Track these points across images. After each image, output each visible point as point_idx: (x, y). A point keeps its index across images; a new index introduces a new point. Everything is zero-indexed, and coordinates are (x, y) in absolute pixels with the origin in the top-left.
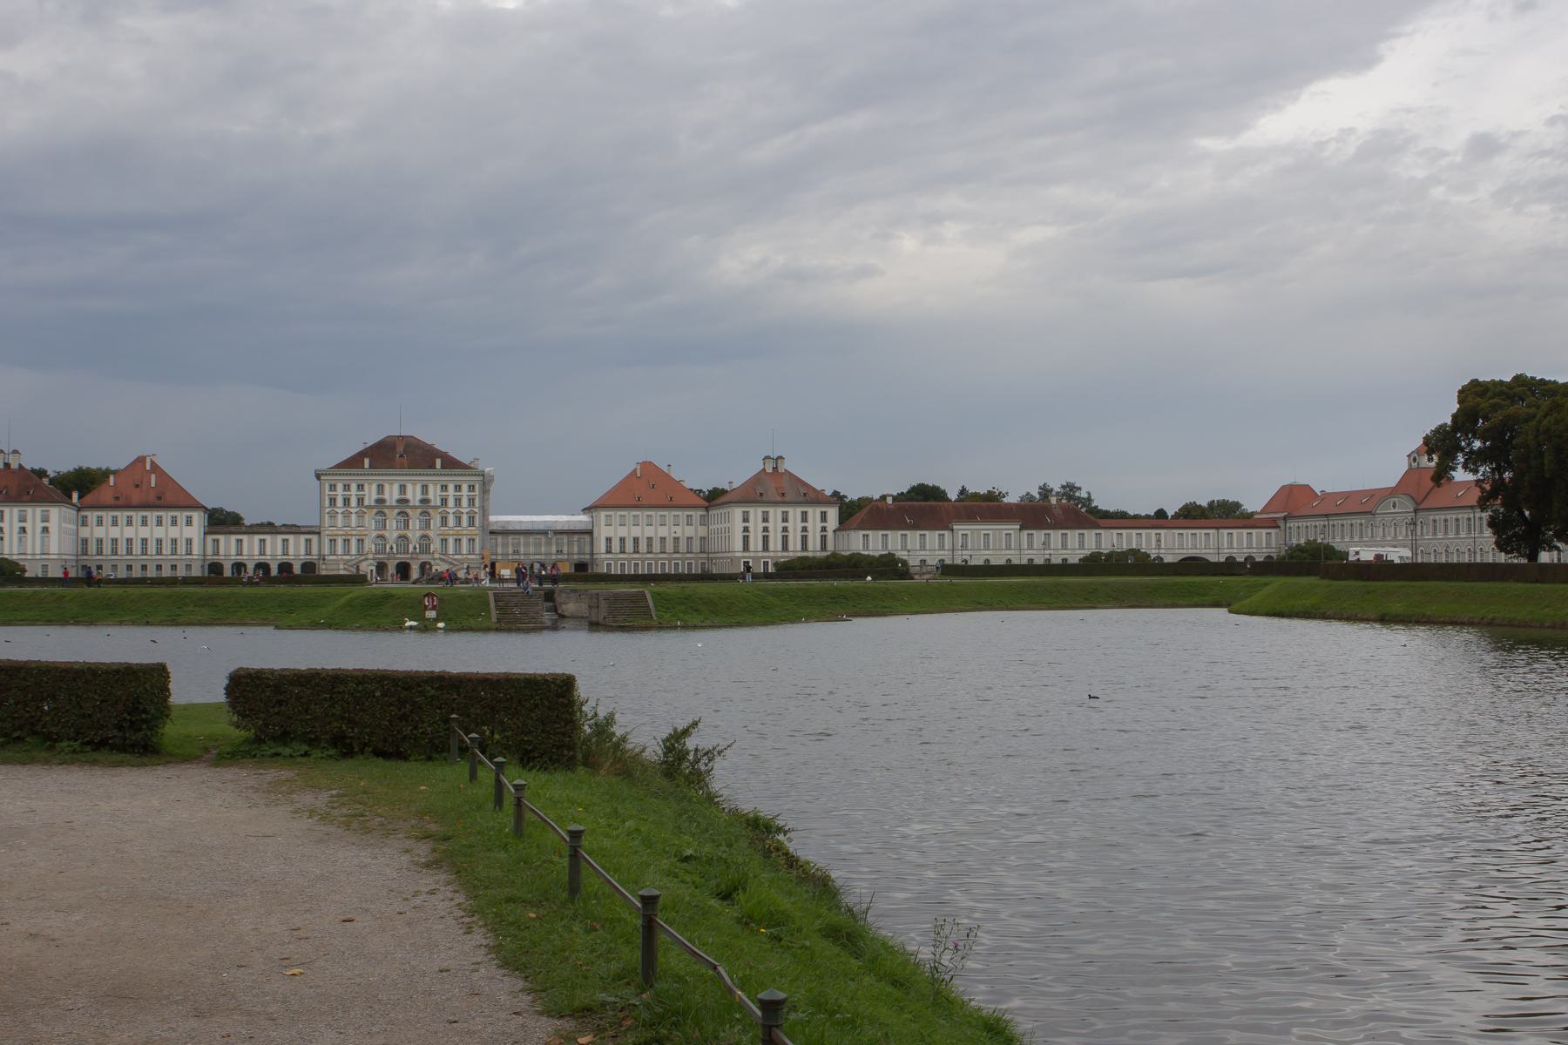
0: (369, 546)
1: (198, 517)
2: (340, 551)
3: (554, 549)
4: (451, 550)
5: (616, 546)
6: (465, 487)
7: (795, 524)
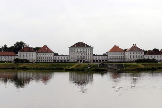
1: (53, 54)
2: (72, 58)
4: (88, 58)
5: (111, 58)
6: (89, 49)
7: (138, 54)
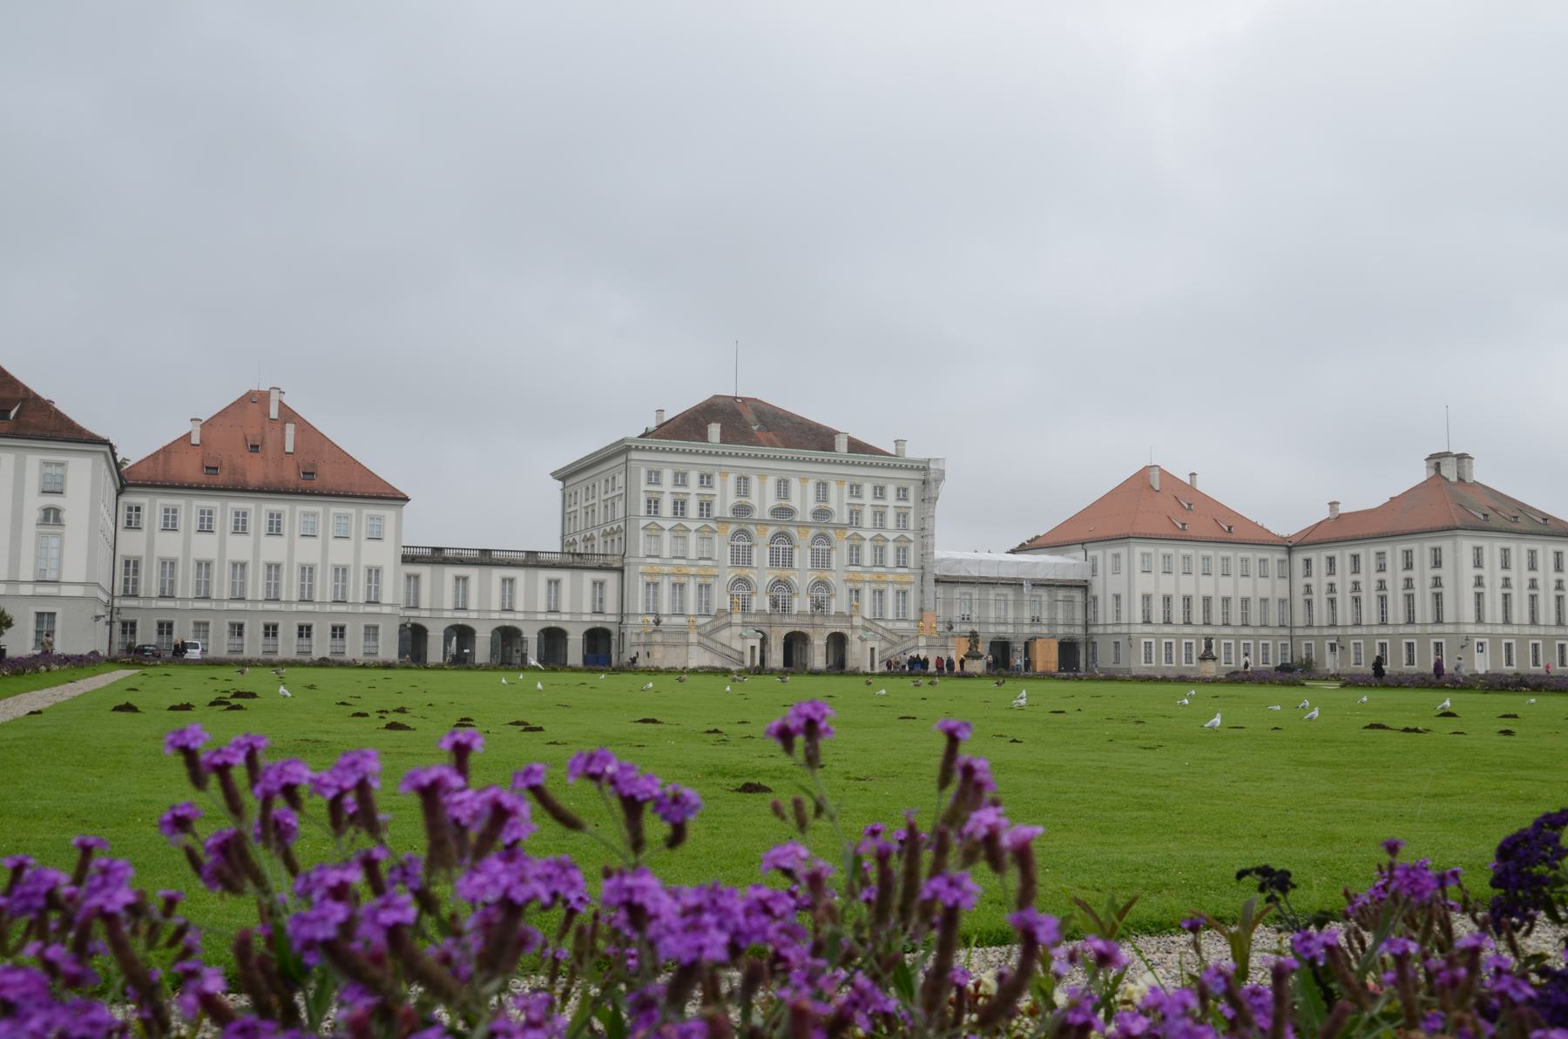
3: (1027, 615)
5: (1157, 614)
6: (891, 491)
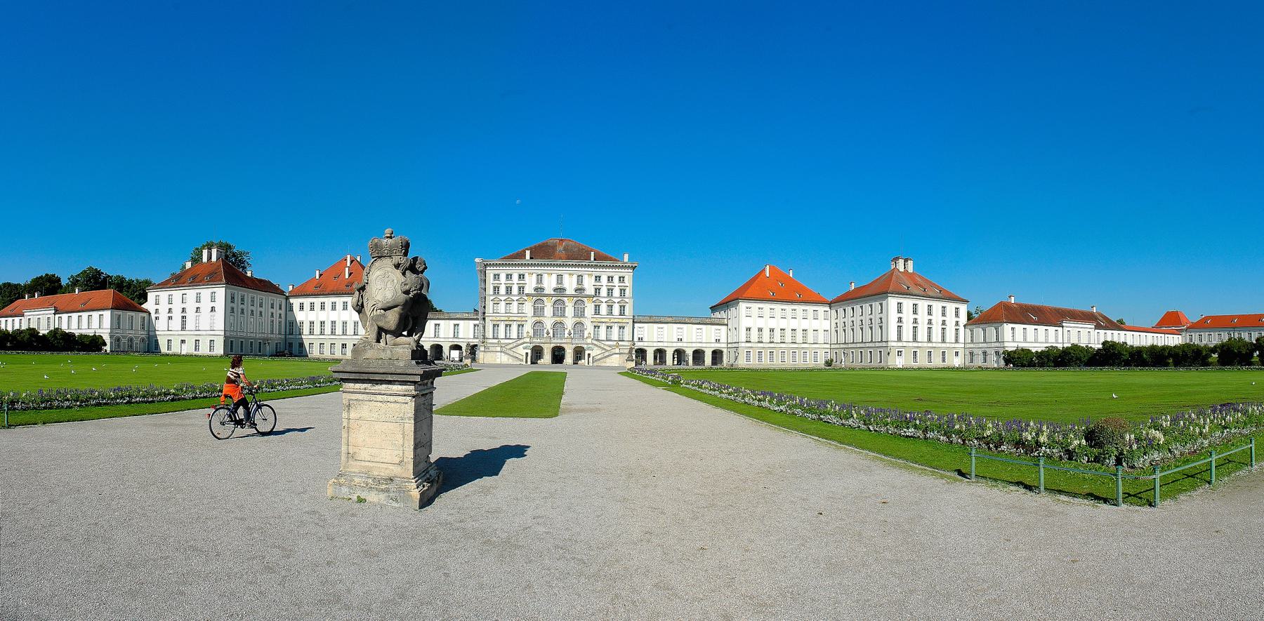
0: (528, 328)
2: (502, 335)
